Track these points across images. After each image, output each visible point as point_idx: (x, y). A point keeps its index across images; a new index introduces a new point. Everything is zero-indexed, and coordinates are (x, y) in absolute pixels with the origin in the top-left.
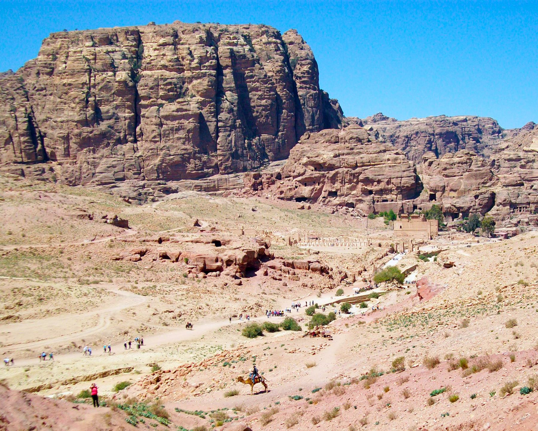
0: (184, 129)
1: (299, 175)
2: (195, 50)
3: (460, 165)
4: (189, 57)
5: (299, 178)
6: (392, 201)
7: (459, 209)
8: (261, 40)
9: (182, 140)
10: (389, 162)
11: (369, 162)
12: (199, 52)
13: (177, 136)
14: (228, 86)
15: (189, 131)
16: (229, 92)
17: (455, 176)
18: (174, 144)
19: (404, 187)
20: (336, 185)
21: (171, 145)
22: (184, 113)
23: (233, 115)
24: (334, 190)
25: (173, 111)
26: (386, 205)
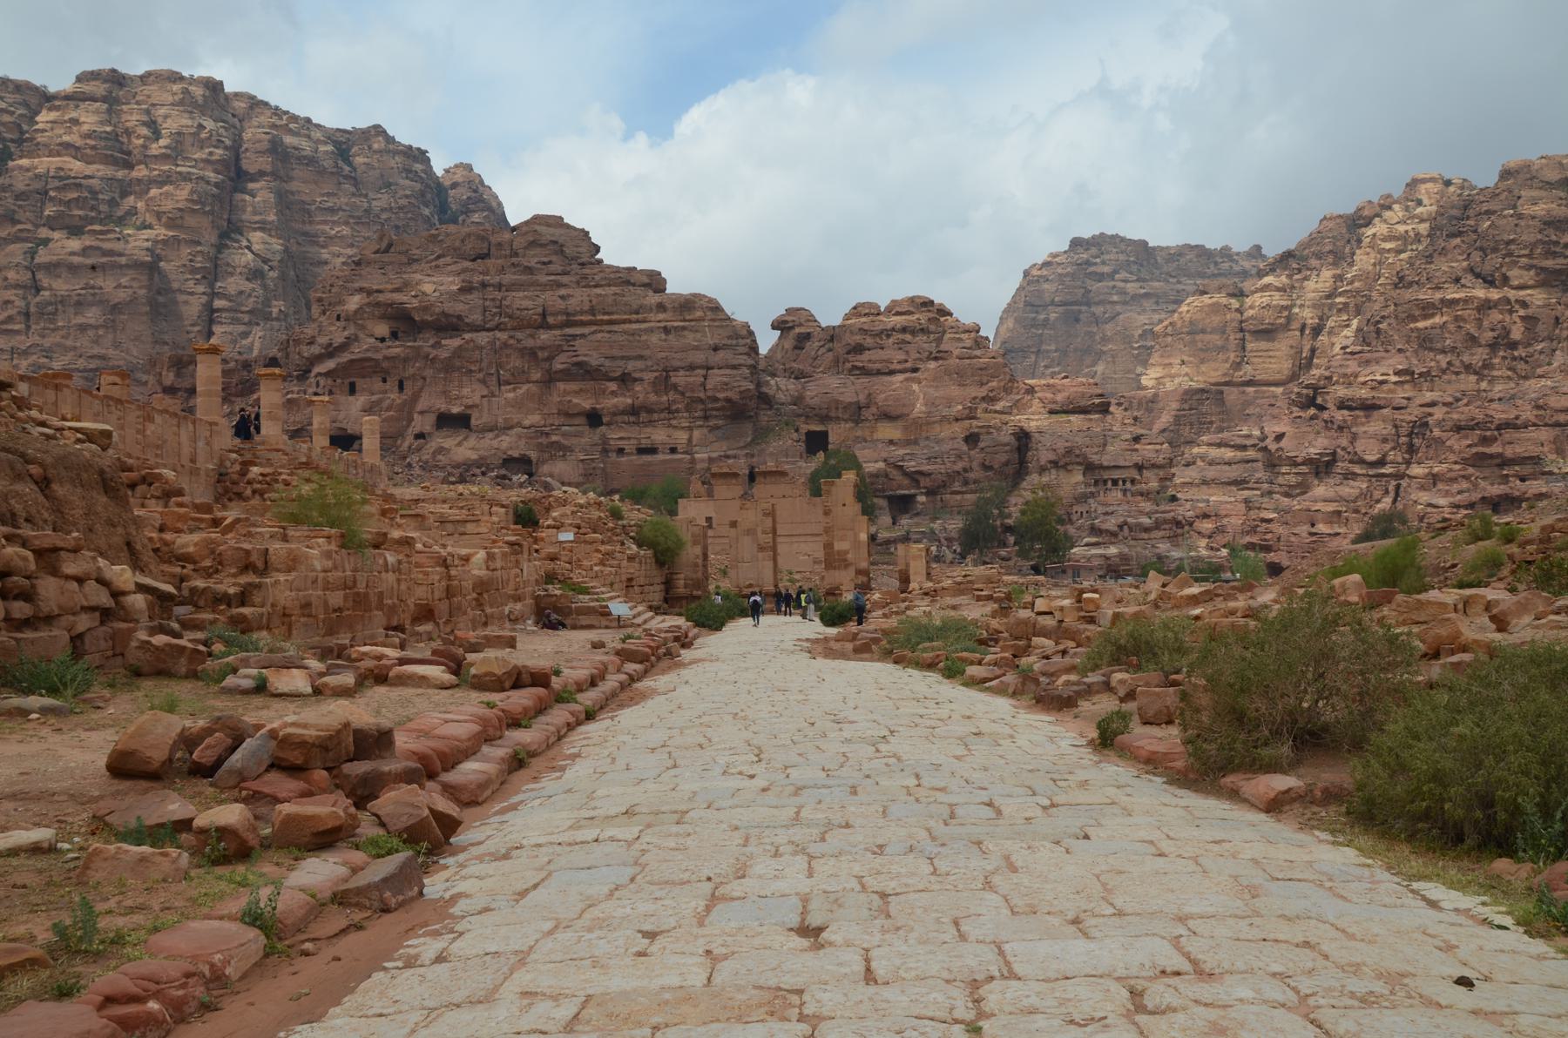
0: (101, 302)
1: (331, 351)
2: (166, 117)
3: (908, 337)
4: (144, 131)
5: (330, 364)
6: (673, 450)
7: (914, 477)
8: (370, 148)
9: (91, 333)
10: (661, 316)
11: (592, 311)
12: (174, 122)
13: (80, 320)
14: (257, 218)
15: (116, 308)
16: (259, 234)
17: (892, 373)
18: (69, 343)
19: (716, 400)
20: (465, 391)
21: (58, 345)
22: (104, 260)
23: (265, 287)
24: (455, 410)
25: (73, 254)
26: (650, 464)
